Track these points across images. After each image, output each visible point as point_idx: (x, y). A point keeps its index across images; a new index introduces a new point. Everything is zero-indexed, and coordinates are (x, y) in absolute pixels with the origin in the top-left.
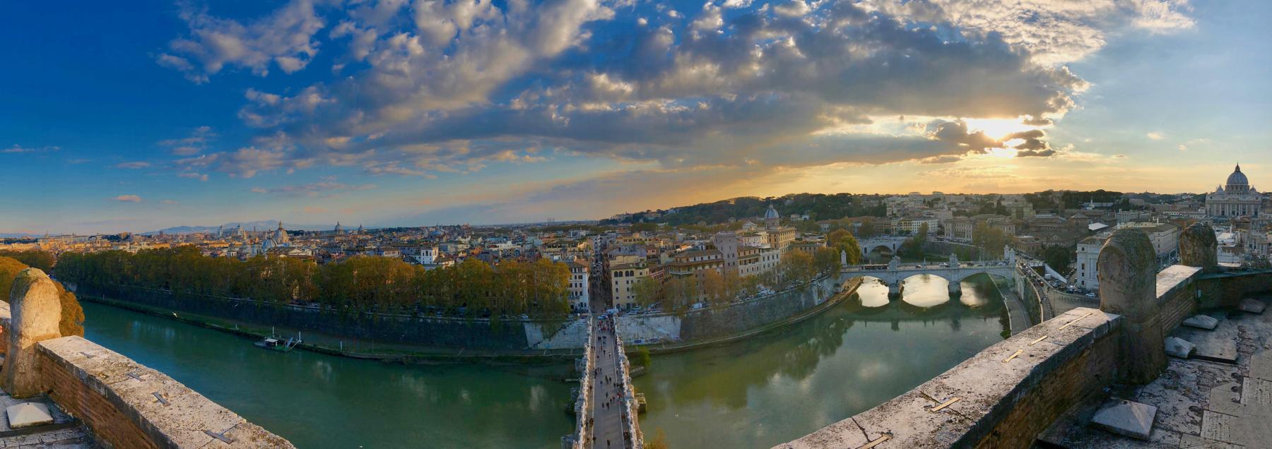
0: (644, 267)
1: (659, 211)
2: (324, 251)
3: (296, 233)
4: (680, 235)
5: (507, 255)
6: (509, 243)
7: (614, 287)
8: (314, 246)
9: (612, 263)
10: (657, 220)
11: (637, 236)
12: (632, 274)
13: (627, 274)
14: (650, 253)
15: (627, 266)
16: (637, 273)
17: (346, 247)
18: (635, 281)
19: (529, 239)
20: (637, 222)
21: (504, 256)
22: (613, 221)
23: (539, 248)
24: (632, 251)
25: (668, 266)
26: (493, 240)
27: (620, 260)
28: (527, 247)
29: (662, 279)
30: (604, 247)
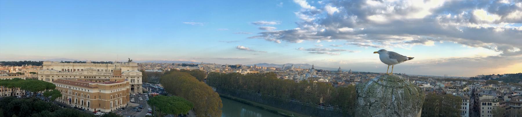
0: (496, 102)
1: (498, 75)
2: (334, 80)
3: (319, 71)
4: (513, 88)
5: (428, 90)
6: (429, 84)
7: (482, 110)
8: (329, 78)
9: (481, 98)
10: (497, 79)
11: (491, 86)
12: (491, 104)
13: (488, 104)
14: (498, 95)
15: (488, 100)
16: (493, 104)
17: (345, 79)
18: (492, 108)
19: (438, 84)
20: (489, 79)
21: (426, 91)
22: (476, 78)
23: (443, 88)
24: (490, 93)
25: (508, 102)
26: (420, 82)
27: (484, 97)
28: (437, 87)
29: (504, 108)
30: (474, 91)
